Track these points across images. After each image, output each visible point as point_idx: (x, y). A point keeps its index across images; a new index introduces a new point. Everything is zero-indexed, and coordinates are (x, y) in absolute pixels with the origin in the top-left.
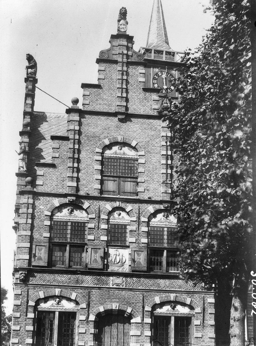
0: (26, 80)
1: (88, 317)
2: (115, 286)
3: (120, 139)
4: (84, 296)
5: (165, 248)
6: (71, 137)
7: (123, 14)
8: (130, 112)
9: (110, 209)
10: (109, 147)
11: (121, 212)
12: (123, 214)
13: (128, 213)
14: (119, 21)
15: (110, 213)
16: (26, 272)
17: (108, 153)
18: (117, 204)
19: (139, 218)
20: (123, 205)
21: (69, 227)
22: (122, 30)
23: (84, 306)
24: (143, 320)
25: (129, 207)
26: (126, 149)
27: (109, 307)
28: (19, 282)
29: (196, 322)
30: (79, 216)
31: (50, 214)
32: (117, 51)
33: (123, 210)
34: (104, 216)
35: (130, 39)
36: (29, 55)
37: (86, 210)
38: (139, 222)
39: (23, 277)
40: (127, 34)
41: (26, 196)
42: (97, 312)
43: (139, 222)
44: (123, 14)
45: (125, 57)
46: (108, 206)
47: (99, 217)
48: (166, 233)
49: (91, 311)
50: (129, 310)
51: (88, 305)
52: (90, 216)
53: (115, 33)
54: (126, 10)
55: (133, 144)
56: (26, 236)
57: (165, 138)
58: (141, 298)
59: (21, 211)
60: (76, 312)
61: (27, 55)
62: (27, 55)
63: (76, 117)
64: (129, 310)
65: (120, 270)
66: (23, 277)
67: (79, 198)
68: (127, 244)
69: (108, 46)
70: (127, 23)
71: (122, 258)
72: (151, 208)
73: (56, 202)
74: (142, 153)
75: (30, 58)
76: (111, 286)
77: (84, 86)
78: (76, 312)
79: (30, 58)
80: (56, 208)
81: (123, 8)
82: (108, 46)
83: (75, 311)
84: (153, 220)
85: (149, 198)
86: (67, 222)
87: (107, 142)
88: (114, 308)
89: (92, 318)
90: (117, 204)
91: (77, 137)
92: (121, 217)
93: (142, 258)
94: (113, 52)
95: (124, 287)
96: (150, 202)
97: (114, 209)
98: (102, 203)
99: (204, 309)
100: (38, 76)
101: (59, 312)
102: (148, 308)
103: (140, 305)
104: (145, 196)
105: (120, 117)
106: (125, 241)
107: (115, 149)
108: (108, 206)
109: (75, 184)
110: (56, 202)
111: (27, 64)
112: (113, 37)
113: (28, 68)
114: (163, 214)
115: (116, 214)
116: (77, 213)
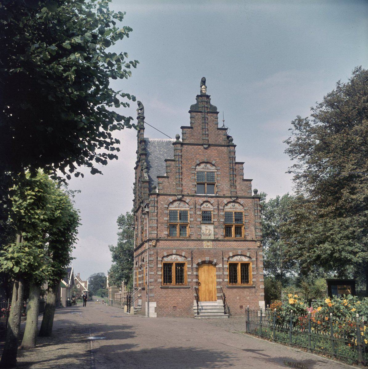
1: (192, 266)
4: (189, 254)
5: (234, 224)
6: (177, 159)
7: (203, 82)
8: (210, 143)
9: (202, 202)
10: (199, 165)
11: (208, 203)
12: (209, 205)
13: (212, 204)
14: (201, 86)
15: (202, 204)
17: (199, 168)
18: (205, 199)
19: (218, 207)
20: (209, 199)
21: (178, 214)
22: (203, 92)
23: (190, 259)
24: (223, 266)
25: (212, 200)
26: (208, 165)
27: (204, 260)
28: (152, 247)
29: (251, 266)
30: (183, 207)
31: (167, 206)
32: (201, 105)
33: (209, 202)
34: (198, 207)
35: (208, 97)
36: (139, 101)
37: (188, 204)
38: (218, 209)
39: (154, 244)
40: (207, 94)
41: (153, 196)
42: (197, 263)
43: (218, 209)
44: (203, 82)
45: (206, 109)
46: (201, 200)
47: (195, 207)
48: (234, 215)
49: (193, 262)
50: (215, 261)
51: (192, 258)
52: (190, 207)
53: (200, 94)
54: (205, 79)
55: (213, 162)
56: (154, 220)
57: (232, 158)
58: (222, 253)
59: (150, 205)
60: (185, 263)
63: (179, 146)
64: (215, 261)
65: (209, 238)
67: (183, 196)
68: (212, 222)
69: (195, 102)
70: (206, 87)
71: (208, 230)
72: (225, 201)
73: (171, 199)
74: (219, 168)
76: (204, 247)
77: (182, 128)
78: (185, 263)
80: (171, 203)
81: (203, 78)
82: (195, 102)
83: (184, 262)
84: (226, 207)
85: (224, 195)
86: (177, 211)
87: (198, 163)
88: (206, 260)
89: (195, 266)
90: (205, 199)
91: (180, 160)
92: (208, 206)
93: (221, 232)
94: (200, 106)
95: (211, 248)
96: (224, 197)
97: (204, 202)
98: (197, 199)
99: (257, 259)
100: (145, 115)
101: (176, 263)
102: (225, 259)
103: (221, 257)
104: (221, 194)
105: (205, 146)
106: (211, 220)
107: (202, 165)
108: (201, 200)
109: (180, 188)
110: (171, 199)
111: (138, 107)
112: (198, 96)
113: (138, 110)
114: (232, 204)
115: (204, 205)
116: (182, 204)
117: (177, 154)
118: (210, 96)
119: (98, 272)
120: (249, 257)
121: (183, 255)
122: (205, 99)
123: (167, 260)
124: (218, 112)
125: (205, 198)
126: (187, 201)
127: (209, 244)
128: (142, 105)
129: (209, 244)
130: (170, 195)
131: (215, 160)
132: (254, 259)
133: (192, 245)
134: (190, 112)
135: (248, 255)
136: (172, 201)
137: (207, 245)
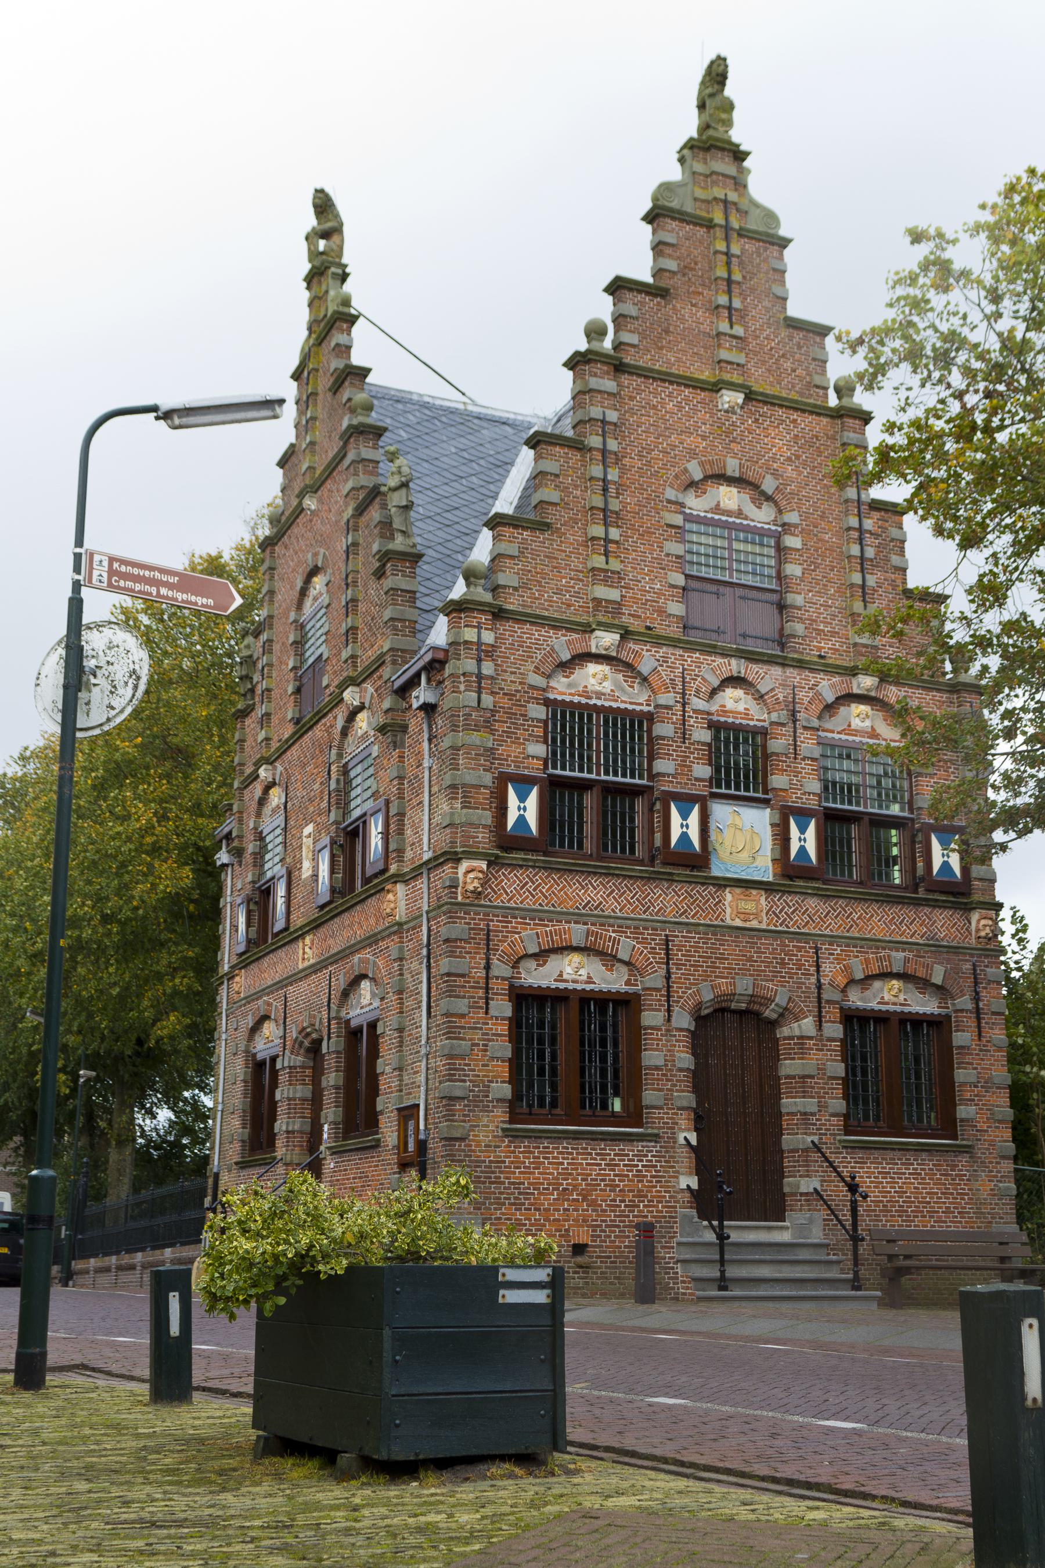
0: (312, 279)
2: (738, 923)
3: (732, 467)
16: (485, 867)
18: (735, 666)
20: (752, 671)
39: (476, 884)
55: (769, 485)
61: (316, 191)
62: (316, 191)
66: (476, 884)
69: (675, 173)
71: (744, 837)
75: (323, 205)
76: (729, 922)
79: (323, 205)
81: (719, 57)
117: (596, 412)
118: (747, 154)
119: (769, 828)
120: (941, 991)
121: (621, 955)
122: (723, 165)
123: (540, 976)
124: (789, 241)
125: (733, 661)
126: (645, 668)
127: (749, 906)
128: (337, 216)
129: (749, 906)
130: (556, 625)
131: (775, 474)
132: (965, 1002)
133: (668, 901)
134: (650, 218)
135: (937, 979)
136: (566, 656)
137: (733, 908)
